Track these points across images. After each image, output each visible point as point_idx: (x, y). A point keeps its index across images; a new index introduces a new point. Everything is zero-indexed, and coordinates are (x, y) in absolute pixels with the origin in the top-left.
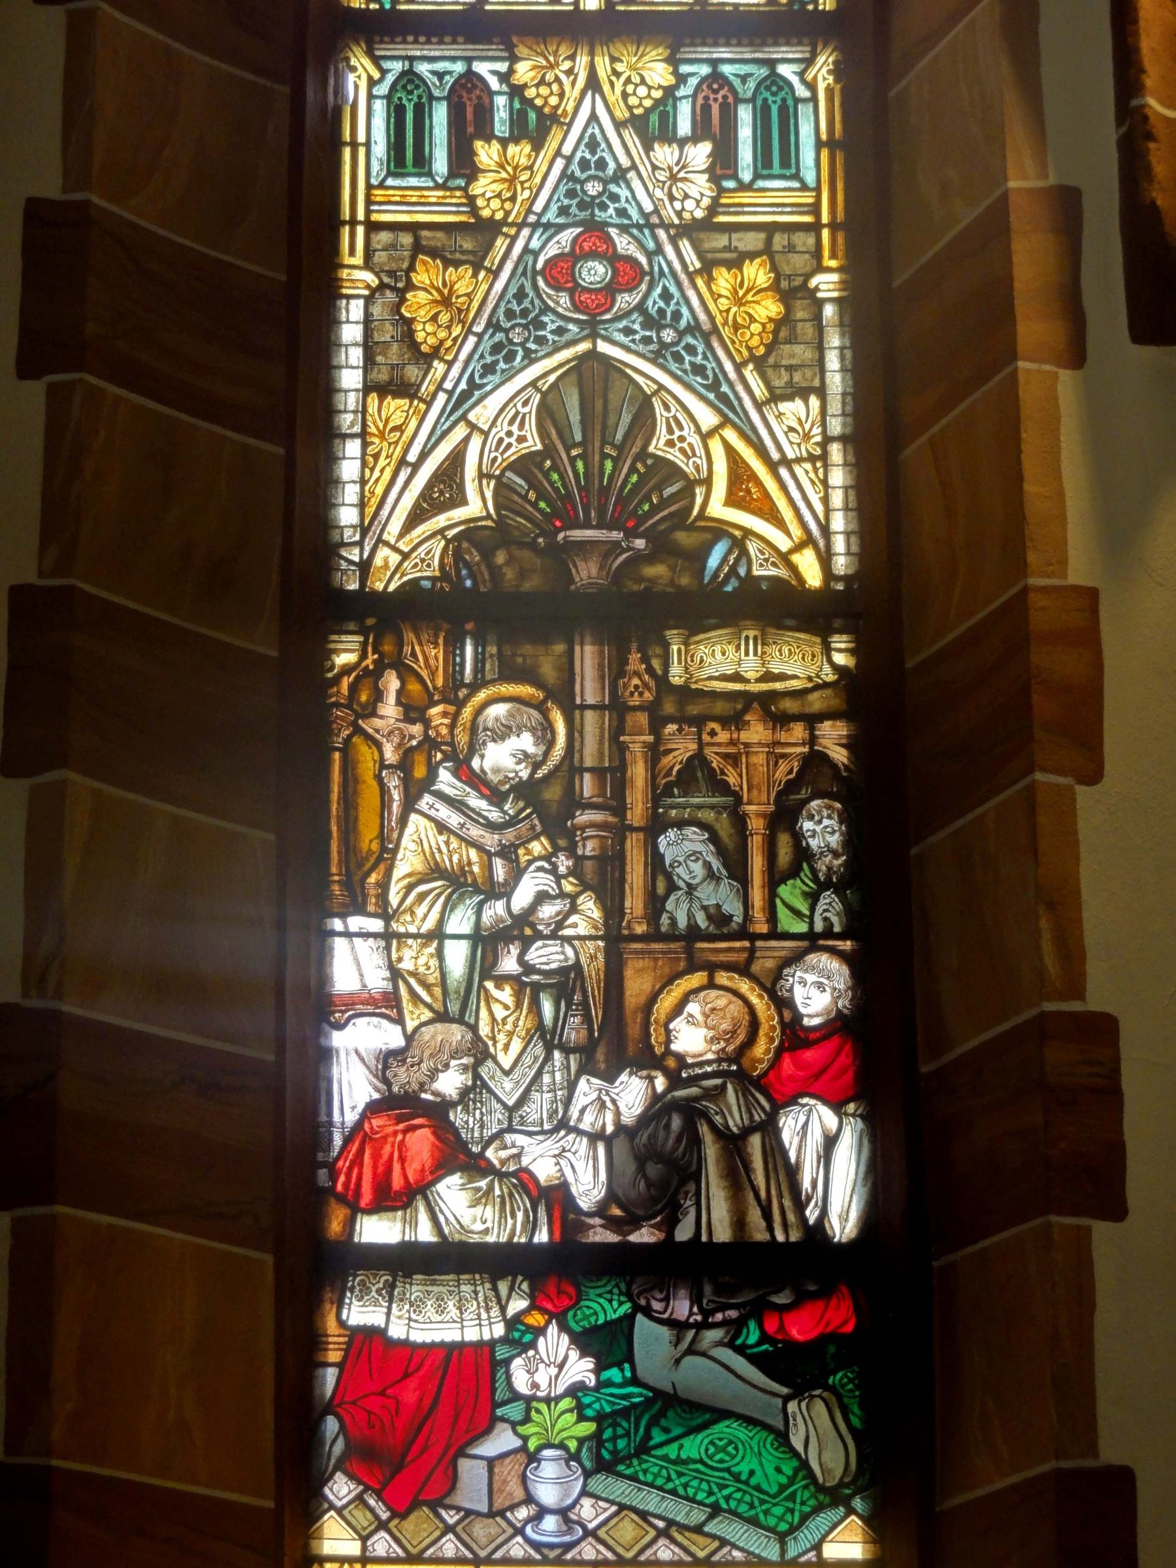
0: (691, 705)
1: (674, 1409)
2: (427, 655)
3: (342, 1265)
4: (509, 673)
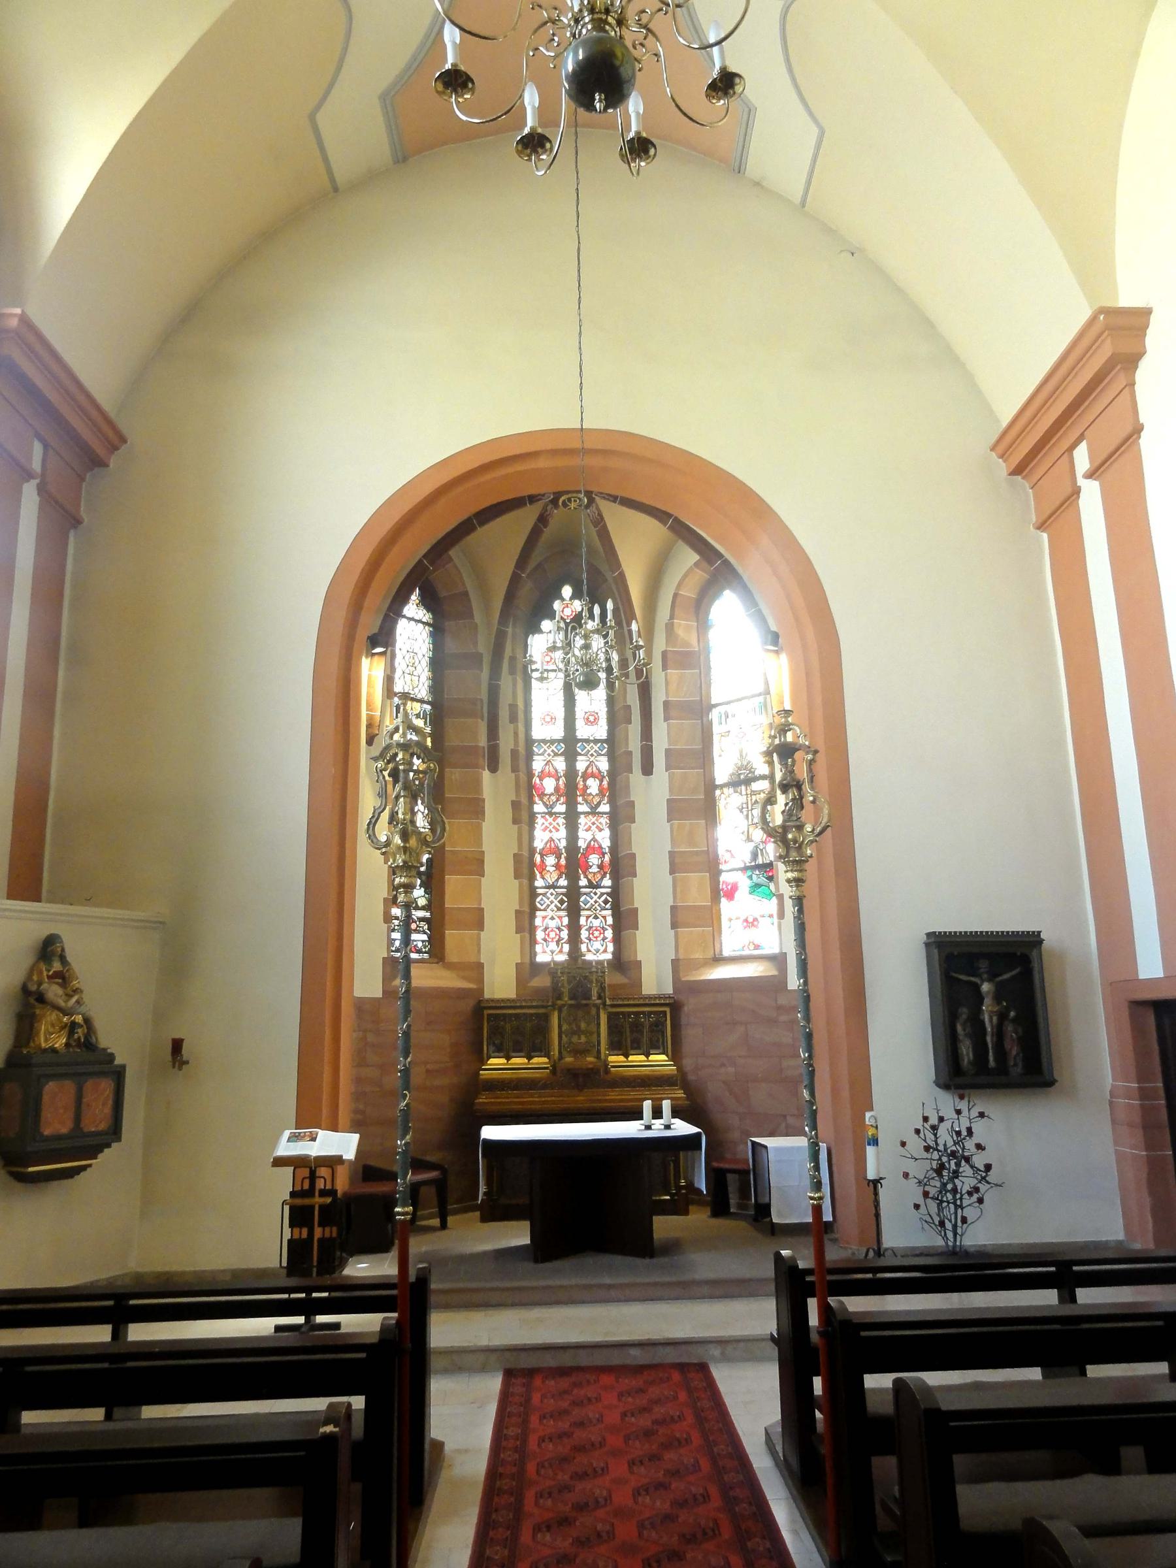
0: (754, 793)
1: (758, 886)
2: (725, 790)
3: (719, 872)
4: (736, 792)
